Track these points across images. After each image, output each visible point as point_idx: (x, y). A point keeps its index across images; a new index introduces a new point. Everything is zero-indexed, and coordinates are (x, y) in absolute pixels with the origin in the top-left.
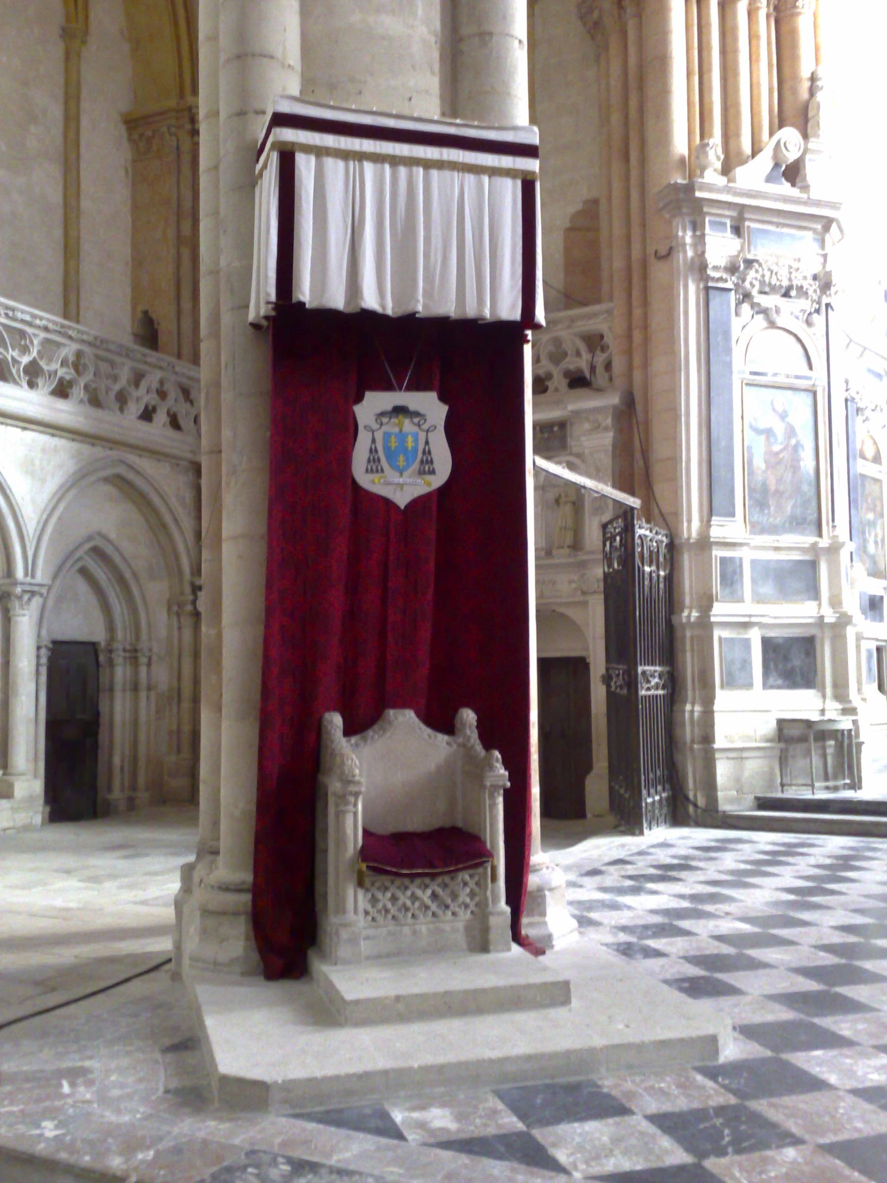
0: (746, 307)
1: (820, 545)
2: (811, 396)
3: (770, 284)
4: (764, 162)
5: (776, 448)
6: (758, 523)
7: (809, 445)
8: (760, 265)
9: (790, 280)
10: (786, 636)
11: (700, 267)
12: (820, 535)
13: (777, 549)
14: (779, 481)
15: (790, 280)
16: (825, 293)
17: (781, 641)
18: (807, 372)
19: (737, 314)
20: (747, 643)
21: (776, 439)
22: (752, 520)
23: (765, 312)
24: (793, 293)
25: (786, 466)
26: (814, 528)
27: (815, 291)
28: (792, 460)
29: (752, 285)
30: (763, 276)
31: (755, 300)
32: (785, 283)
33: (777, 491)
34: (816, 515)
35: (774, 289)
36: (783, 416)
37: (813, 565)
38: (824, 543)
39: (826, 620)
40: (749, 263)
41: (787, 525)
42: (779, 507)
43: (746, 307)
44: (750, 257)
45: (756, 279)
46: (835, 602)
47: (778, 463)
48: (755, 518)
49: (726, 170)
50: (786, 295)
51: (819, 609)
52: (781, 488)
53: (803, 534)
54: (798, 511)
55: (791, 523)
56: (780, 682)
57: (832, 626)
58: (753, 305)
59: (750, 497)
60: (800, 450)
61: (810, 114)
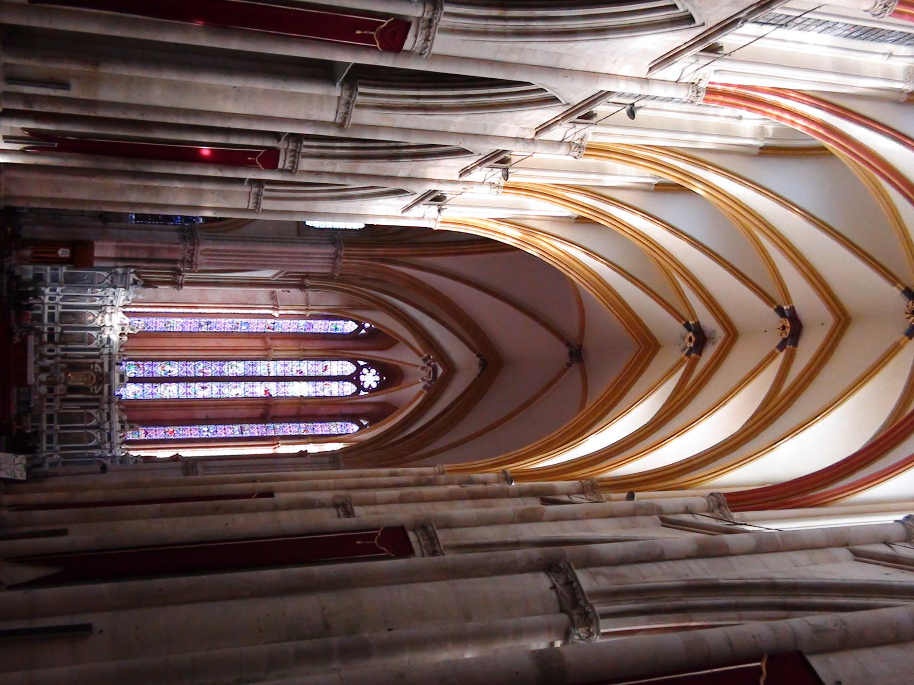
0: (108, 274)
4: (136, 278)
11: (117, 267)
20: (42, 271)
23: (108, 277)
36: (88, 279)
38: (62, 284)
40: (117, 275)
43: (108, 274)
49: (135, 272)
50: (112, 281)
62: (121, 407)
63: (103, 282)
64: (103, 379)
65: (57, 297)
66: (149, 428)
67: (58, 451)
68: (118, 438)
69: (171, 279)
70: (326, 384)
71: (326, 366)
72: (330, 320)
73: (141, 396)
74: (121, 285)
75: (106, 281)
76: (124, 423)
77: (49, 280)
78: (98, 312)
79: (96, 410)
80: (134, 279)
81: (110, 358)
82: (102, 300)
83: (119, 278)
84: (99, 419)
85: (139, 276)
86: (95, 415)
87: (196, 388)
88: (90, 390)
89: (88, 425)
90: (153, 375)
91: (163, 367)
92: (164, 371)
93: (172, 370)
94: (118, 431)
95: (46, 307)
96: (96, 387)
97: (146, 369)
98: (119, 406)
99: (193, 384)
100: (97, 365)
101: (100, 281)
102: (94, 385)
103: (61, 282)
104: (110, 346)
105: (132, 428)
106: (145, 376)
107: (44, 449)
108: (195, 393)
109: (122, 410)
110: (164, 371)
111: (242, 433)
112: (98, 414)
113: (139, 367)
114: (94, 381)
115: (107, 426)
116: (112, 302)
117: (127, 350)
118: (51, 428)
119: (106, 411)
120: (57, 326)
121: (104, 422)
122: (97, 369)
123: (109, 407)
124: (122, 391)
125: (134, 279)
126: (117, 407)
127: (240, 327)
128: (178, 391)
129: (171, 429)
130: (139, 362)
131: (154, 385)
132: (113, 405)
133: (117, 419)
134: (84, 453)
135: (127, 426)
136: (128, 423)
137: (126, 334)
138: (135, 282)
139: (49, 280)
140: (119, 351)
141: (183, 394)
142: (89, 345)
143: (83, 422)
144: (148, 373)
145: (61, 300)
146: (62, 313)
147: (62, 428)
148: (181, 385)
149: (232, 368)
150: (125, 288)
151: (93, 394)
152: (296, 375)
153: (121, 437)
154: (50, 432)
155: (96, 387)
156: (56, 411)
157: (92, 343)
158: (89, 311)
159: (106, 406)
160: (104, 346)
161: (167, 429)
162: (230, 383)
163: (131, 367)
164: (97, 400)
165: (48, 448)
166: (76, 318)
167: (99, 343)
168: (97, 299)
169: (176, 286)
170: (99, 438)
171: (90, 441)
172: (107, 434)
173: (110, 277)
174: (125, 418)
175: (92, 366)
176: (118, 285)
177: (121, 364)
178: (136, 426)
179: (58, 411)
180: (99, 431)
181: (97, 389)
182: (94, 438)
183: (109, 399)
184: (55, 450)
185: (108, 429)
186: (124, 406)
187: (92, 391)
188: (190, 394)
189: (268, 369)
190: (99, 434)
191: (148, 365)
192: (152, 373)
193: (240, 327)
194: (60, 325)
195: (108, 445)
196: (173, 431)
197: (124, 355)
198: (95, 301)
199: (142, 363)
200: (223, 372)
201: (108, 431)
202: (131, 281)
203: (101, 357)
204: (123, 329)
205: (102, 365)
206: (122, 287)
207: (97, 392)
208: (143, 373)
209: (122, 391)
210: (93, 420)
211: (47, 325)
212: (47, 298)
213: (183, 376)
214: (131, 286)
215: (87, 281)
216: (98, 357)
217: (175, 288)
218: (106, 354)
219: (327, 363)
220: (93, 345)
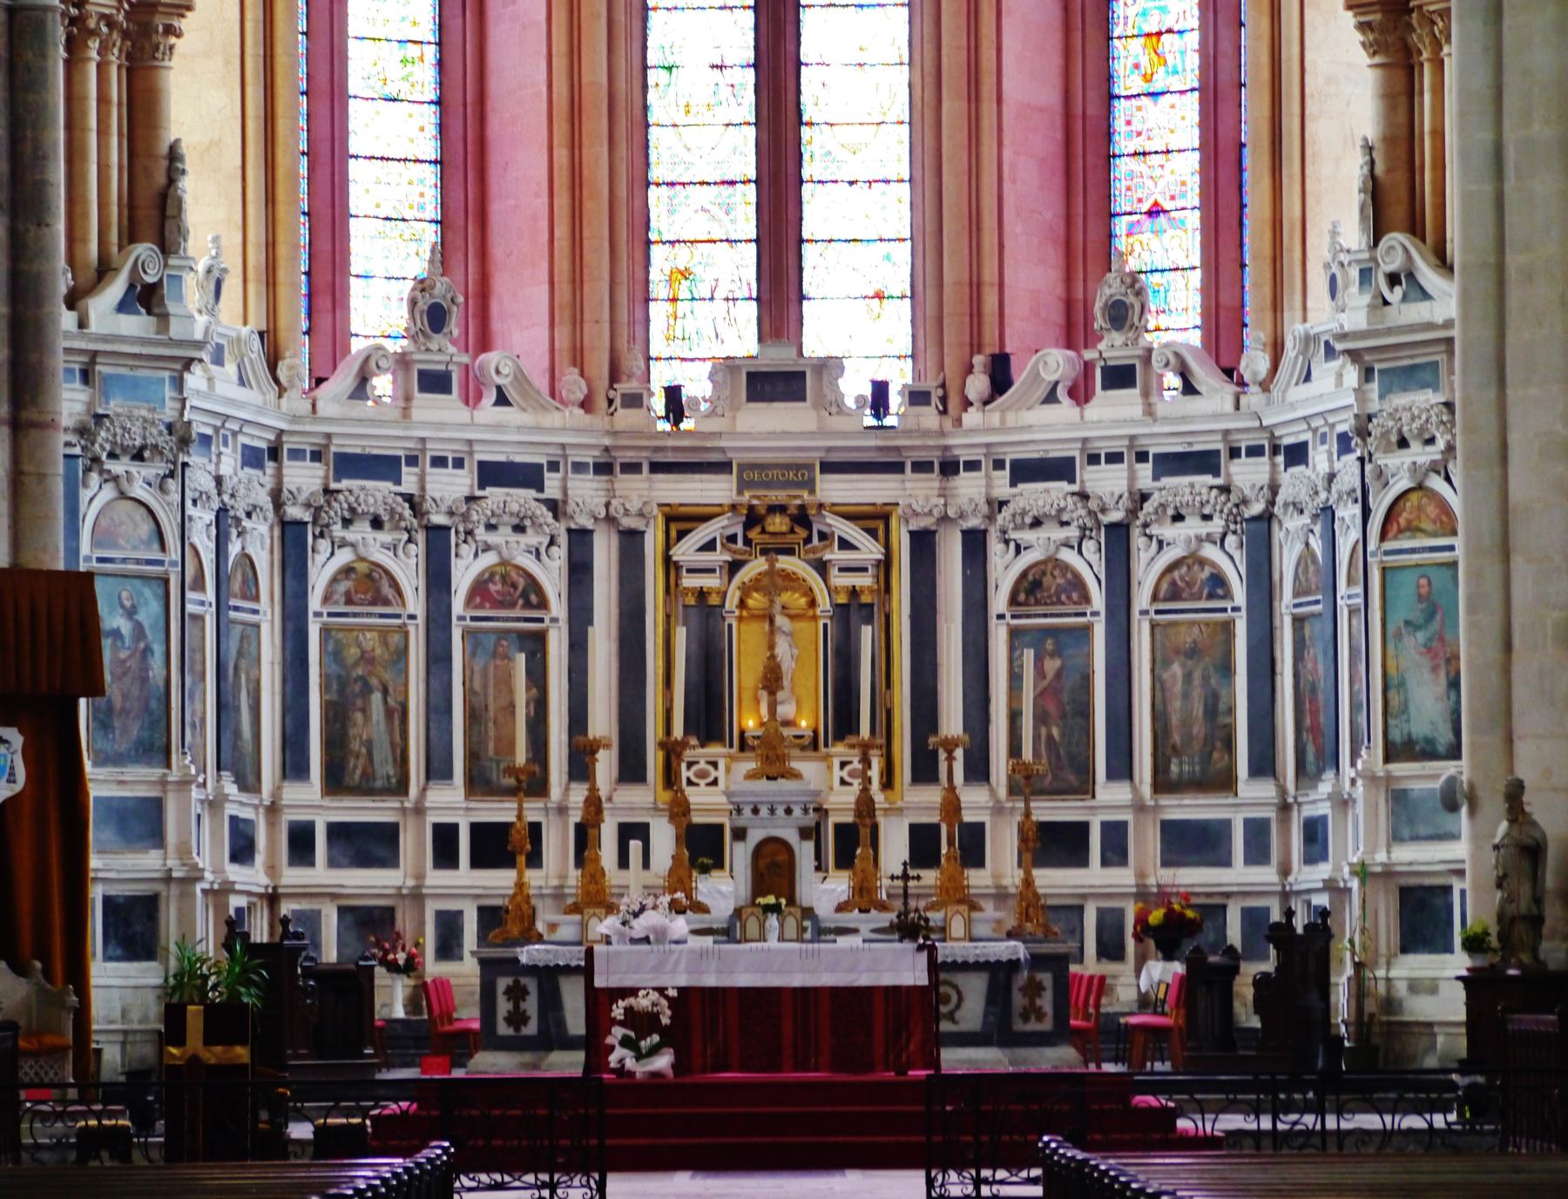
0: (94, 478)
1: (170, 779)
2: (162, 585)
3: (122, 445)
4: (116, 289)
5: (123, 655)
6: (101, 751)
7: (158, 649)
8: (112, 422)
9: (144, 438)
10: (127, 893)
12: (169, 766)
13: (121, 782)
14: (125, 697)
15: (144, 438)
16: (182, 450)
17: (121, 900)
18: (156, 555)
19: (86, 485)
21: (123, 643)
22: (96, 747)
24: (147, 454)
25: (133, 678)
26: (161, 756)
27: (171, 449)
28: (141, 670)
29: (102, 447)
30: (115, 435)
31: (106, 467)
32: (137, 443)
33: (123, 709)
34: (164, 739)
35: (125, 449)
36: (130, 613)
37: (157, 805)
38: (174, 775)
39: (175, 874)
40: (99, 418)
41: (133, 753)
42: (125, 730)
43: (94, 478)
44: (100, 411)
45: (107, 440)
46: (184, 851)
47: (125, 674)
48: (99, 746)
49: (73, 300)
50: (138, 456)
51: (165, 859)
52: (128, 705)
53: (150, 764)
54: (146, 734)
55: (137, 751)
56: (119, 952)
57: (181, 880)
58: (101, 472)
59: (95, 718)
60: (149, 655)
61: (170, 211)
62: (978, 384)
63: (151, 512)
64: (781, 509)
65: (230, 810)
67: (1283, 791)
68: (1193, 405)
69: (114, 57)
73: (888, 257)
74: (169, 392)
75: (139, 491)
76: (1088, 367)
77: (149, 862)
78: (324, 545)
79: (995, 547)
80: (123, 307)
81: (632, 468)
82: (246, 523)
83: (114, 406)
84: (1060, 534)
85: (105, 270)
86: (1027, 559)
88: (854, 592)
89: (1098, 600)
94: (1149, 411)
95: (294, 877)
96: (835, 555)
98: (967, 404)
100: (685, 551)
101: (146, 527)
102: (822, 568)
103: (163, 783)
104: (554, 467)
105: (1119, 315)
107: (1266, 875)
109: (1000, 379)
112: (1026, 536)
113: (685, 274)
114: (785, 563)
115: (1108, 482)
116: (252, 458)
117: (578, 358)
118: (1115, 836)
119: (1001, 484)
120: (419, 811)
121: (1084, 496)
122: (709, 546)
123: (973, 466)
124: (854, 386)
125: (123, 307)
126: (972, 417)
129: (1128, 56)
130: (654, 274)
132: (962, 444)
133: (1066, 409)
134: (1298, 621)
135: (1112, 347)
136: (1091, 339)
137: (465, 359)
138: (145, 297)
139: (149, 862)
140: (586, 405)
142: (543, 604)
143: (1087, 630)
145: (248, 782)
146: (335, 783)
147: (1121, 768)
150: (188, 363)
151: (885, 566)
153: (1189, 389)
154: (1146, 844)
155: (835, 555)
156: (998, 810)
157: (533, 584)
158: (315, 602)
159: (969, 488)
160: (554, 507)
161: (1126, 81)
163: (689, 326)
164: (923, 543)
165: (1257, 852)
166: (367, 690)
167: (532, 538)
168: (234, 549)
169: (160, 22)
170: (1193, 527)
171: (1218, 583)
172: (1168, 481)
173: (117, 467)
174: (1056, 363)
175: (689, 581)
176: (169, 413)
177: (673, 393)
178: (1110, 289)
179: (1002, 792)
180: (1146, 525)
181: (845, 545)
182: (1193, 560)
183: (921, 467)
184: (1270, 813)
185: (1132, 477)
186: (970, 369)
187: (864, 581)
190: (1168, 531)
192: (733, 183)
194: (413, 790)
195: (1248, 474)
197: (614, 376)
198: (247, 560)
199: (656, 251)
201: (1145, 470)
202: (136, 325)
203: (628, 522)
204: (435, 382)
205: (680, 521)
206: (179, 384)
207: (870, 550)
209: (854, 386)
210: (1066, 568)
211: (420, 876)
212: (236, 873)
214: (176, 330)
215: (149, 611)
216: (631, 541)
217: (170, 30)
218: (611, 493)
220: (552, 576)
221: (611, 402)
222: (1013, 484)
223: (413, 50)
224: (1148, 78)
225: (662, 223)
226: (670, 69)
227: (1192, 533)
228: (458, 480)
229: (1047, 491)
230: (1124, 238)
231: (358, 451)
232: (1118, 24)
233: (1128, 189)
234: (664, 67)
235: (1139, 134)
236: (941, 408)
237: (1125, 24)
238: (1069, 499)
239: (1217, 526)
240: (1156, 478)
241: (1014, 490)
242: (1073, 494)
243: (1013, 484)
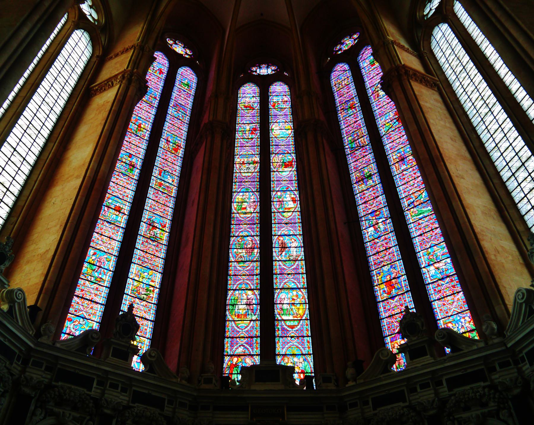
66: (387, 333)
70: (274, 106)
71: (245, 107)
72: (173, 85)
73: (305, 360)
87: (284, 259)
90: (257, 337)
91: (238, 316)
92: (246, 315)
93: (245, 301)
97: (240, 350)
98: (347, 381)
99: (277, 266)
106: (258, 351)
108: (296, 260)
110: (246, 315)
111: (371, 175)
127: (167, 184)
128: (292, 289)
130: (225, 365)
131: (279, 333)
140: (189, 380)
141: (298, 280)
144: (251, 345)
148: (278, 282)
149: (245, 208)
152: (259, 134)
162: (273, 210)
172: (456, 390)
185: (437, 394)
188: (296, 269)
189: (249, 164)
191: (232, 346)
192: (252, 337)
193: (167, 184)
196: (389, 283)
199: (227, 359)
200: (252, 219)
208: (252, 356)
213: (259, 281)
219: (240, 106)
221: (199, 381)
222: (374, 409)
223: (152, 289)
224: (389, 293)
225: (228, 350)
226: (233, 305)
227: (479, 412)
228: (121, 397)
229: (392, 408)
230: (390, 343)
231: (72, 370)
232: (375, 282)
233: (389, 327)
234: (231, 305)
235: (389, 310)
236: (336, 384)
237: (378, 281)
238: (405, 409)
239: (492, 406)
240: (450, 390)
241: (375, 412)
242: (406, 407)
243: (374, 409)
